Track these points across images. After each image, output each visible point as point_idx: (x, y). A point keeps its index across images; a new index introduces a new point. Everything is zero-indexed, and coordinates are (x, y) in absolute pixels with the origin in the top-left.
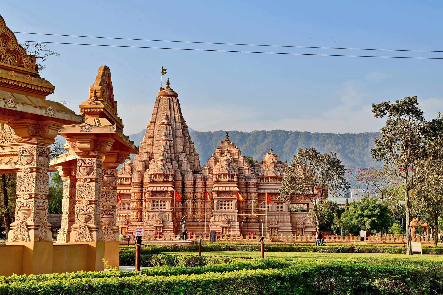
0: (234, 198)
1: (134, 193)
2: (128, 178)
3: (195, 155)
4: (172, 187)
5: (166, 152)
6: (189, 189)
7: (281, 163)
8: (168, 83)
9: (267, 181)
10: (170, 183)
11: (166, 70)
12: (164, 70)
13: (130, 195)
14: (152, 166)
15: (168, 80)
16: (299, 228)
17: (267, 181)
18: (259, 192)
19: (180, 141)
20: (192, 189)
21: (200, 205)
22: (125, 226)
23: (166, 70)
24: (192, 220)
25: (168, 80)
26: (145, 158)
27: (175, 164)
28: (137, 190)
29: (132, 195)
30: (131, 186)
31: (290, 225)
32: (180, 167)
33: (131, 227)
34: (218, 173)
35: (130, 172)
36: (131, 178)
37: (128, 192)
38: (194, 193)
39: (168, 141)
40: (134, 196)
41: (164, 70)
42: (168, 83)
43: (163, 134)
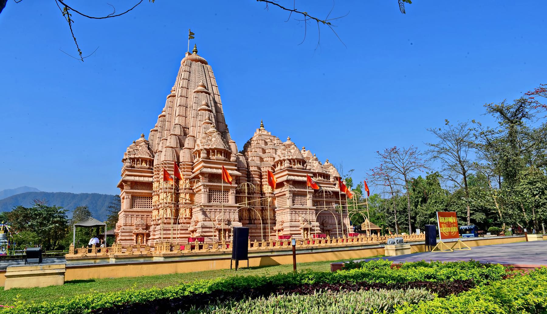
4: (236, 170)
10: (232, 165)
11: (194, 34)
12: (192, 34)
13: (149, 185)
14: (188, 143)
20: (247, 179)
22: (144, 231)
23: (194, 34)
24: (248, 222)
26: (178, 131)
33: (165, 232)
35: (148, 151)
36: (151, 162)
37: (146, 179)
41: (192, 34)
43: (204, 102)
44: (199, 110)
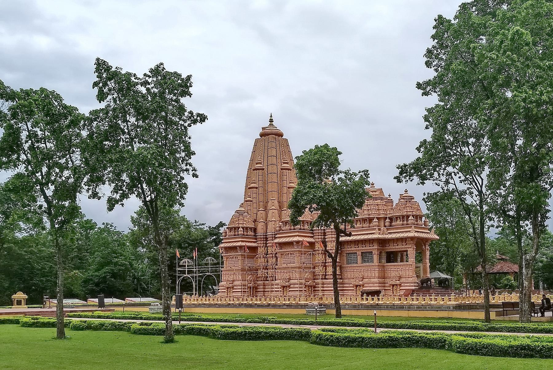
8: (271, 121)
15: (271, 117)
25: (271, 117)
27: (261, 214)
42: (271, 121)
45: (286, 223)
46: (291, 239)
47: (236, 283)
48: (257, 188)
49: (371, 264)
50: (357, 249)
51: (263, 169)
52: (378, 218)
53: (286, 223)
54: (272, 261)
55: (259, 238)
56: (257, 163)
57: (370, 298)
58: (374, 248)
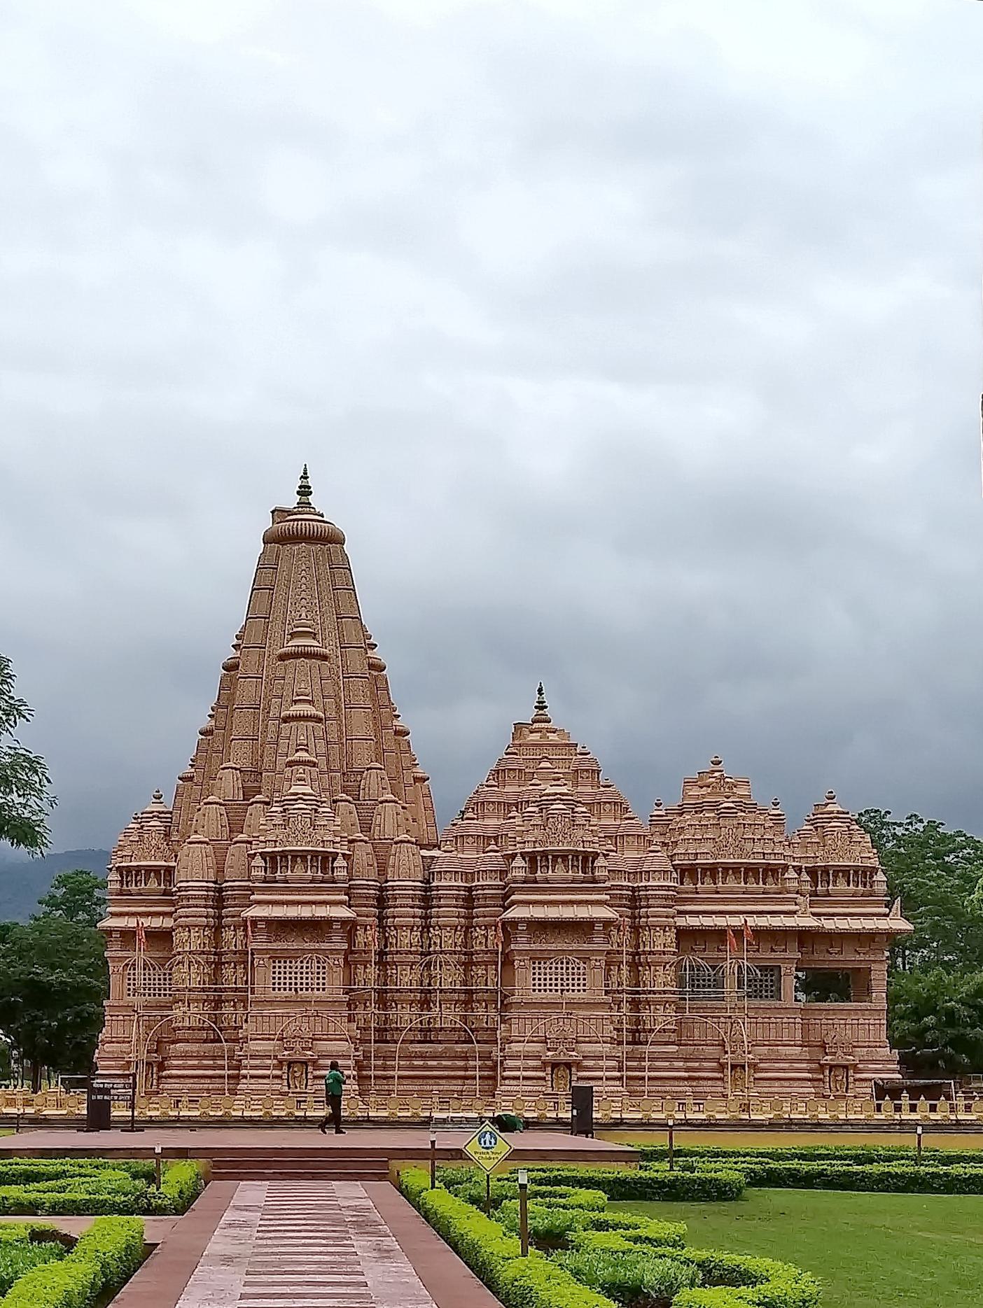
0: (595, 947)
1: (188, 927)
2: (156, 870)
3: (416, 779)
5: (315, 765)
6: (404, 913)
7: (763, 811)
8: (305, 491)
9: (707, 879)
15: (305, 477)
16: (832, 1067)
17: (707, 879)
18: (681, 922)
19: (360, 723)
21: (448, 978)
25: (305, 477)
28: (200, 913)
29: (178, 937)
30: (172, 903)
31: (805, 1053)
32: (366, 827)
34: (529, 849)
38: (426, 928)
39: (319, 720)
40: (190, 941)
42: (305, 491)
44: (286, 720)
45: (555, 858)
46: (582, 913)
47: (323, 1046)
48: (319, 720)
49: (774, 1003)
50: (783, 955)
51: (325, 658)
52: (798, 870)
53: (555, 858)
54: (485, 978)
55: (361, 896)
56: (293, 635)
57: (923, 1103)
58: (787, 955)
